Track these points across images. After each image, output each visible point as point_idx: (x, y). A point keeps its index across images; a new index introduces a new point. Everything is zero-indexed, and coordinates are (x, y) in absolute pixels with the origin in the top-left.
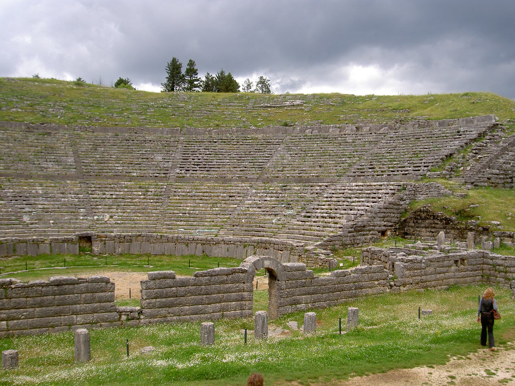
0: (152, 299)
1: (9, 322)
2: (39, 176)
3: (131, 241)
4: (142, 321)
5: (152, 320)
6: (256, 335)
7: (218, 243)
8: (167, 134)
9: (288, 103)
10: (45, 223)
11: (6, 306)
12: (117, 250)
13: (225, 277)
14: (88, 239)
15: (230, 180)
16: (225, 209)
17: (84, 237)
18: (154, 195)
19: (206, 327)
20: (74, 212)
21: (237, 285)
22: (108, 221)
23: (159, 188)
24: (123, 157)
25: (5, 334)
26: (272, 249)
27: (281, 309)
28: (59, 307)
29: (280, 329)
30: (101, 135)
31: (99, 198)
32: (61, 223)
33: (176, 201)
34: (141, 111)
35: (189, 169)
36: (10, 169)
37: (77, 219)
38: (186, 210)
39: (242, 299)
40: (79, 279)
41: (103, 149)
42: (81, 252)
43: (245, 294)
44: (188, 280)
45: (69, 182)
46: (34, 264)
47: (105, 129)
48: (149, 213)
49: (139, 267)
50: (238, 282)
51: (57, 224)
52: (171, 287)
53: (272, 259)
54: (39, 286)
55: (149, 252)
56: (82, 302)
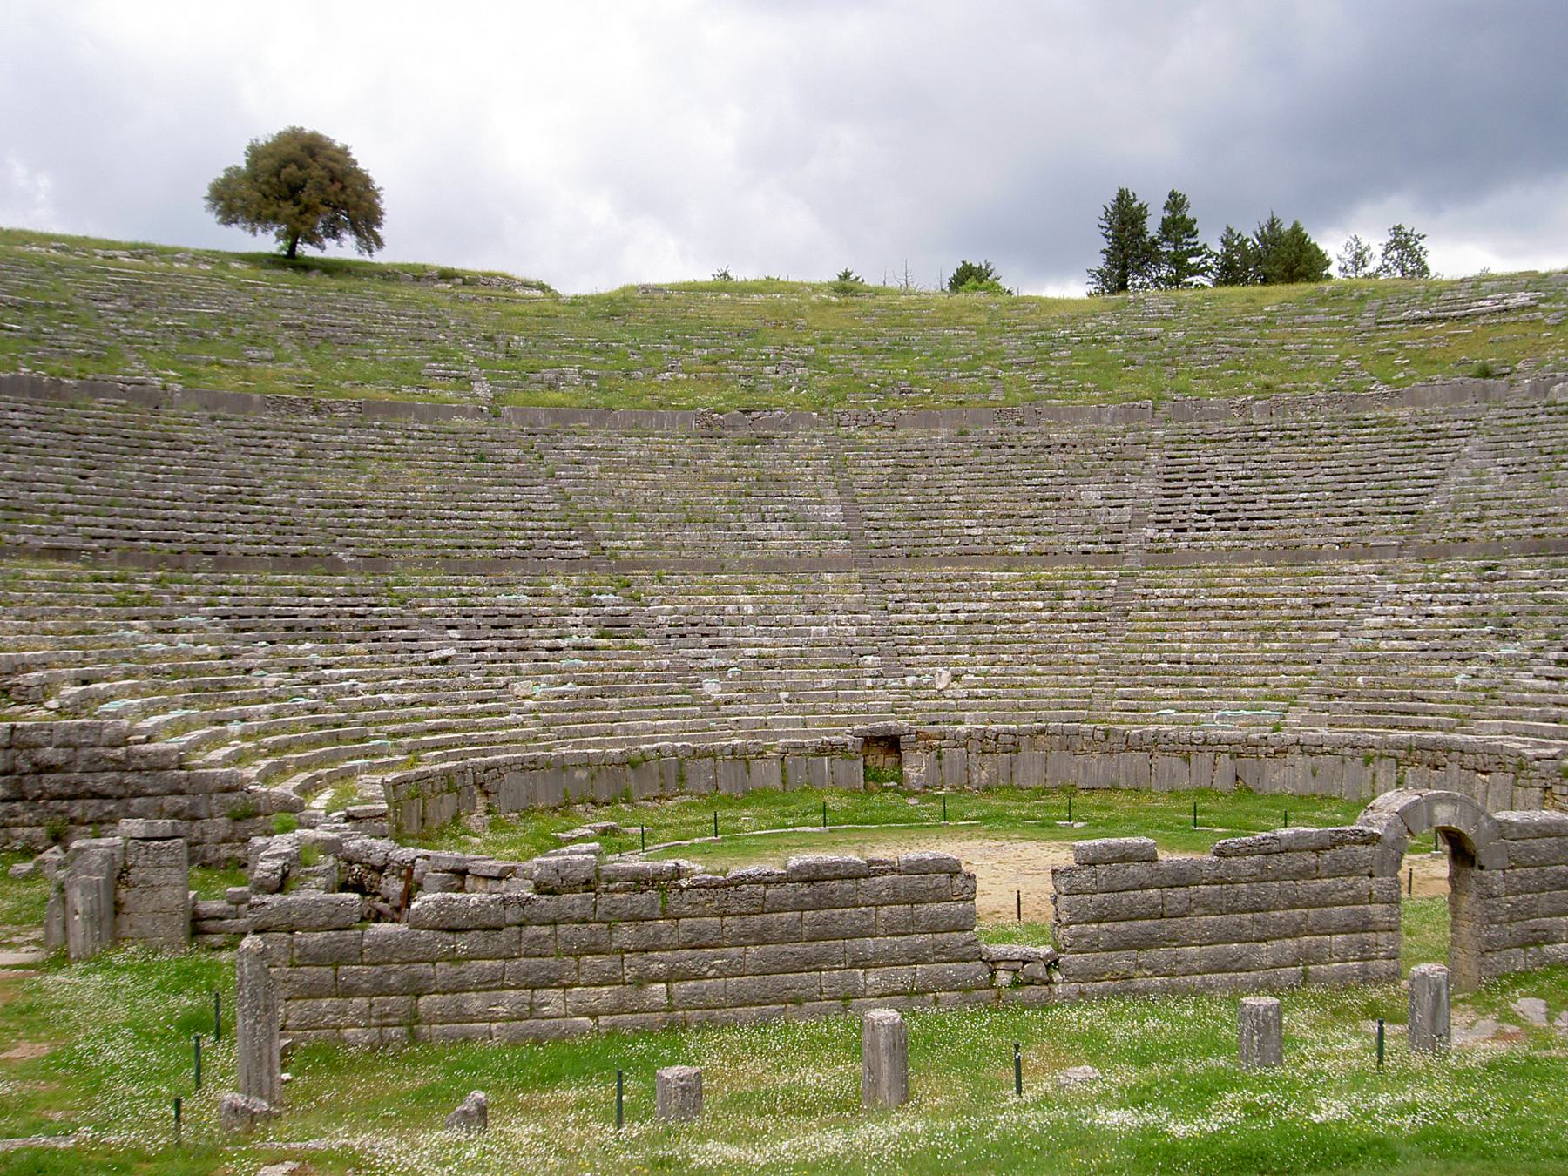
0: (1087, 922)
2: (744, 563)
3: (1016, 748)
4: (1058, 989)
5: (1088, 987)
6: (1412, 1039)
7: (1281, 751)
8: (1113, 423)
9: (1488, 303)
10: (764, 700)
12: (975, 776)
13: (1311, 858)
14: (890, 743)
15: (1315, 555)
16: (1300, 646)
17: (877, 740)
18: (1082, 609)
19: (1254, 1013)
20: (848, 666)
21: (1350, 881)
22: (947, 689)
23: (1095, 587)
24: (985, 497)
25: (664, 1022)
26: (1455, 767)
27: (1492, 958)
28: (814, 945)
29: (1488, 1023)
30: (917, 434)
31: (919, 623)
32: (809, 697)
33: (1153, 625)
34: (1032, 358)
35: (1185, 525)
36: (660, 547)
37: (856, 686)
38: (1180, 651)
39: (1366, 925)
40: (871, 863)
41: (924, 477)
42: (871, 784)
43: (1376, 910)
44: (1196, 867)
45: (829, 577)
46: (737, 819)
47: (927, 418)
48: (1067, 662)
49: (1043, 826)
50: (1351, 872)
51: (798, 701)
52: (1143, 887)
53: (1461, 800)
54: (758, 882)
55: (1071, 781)
56: (881, 931)
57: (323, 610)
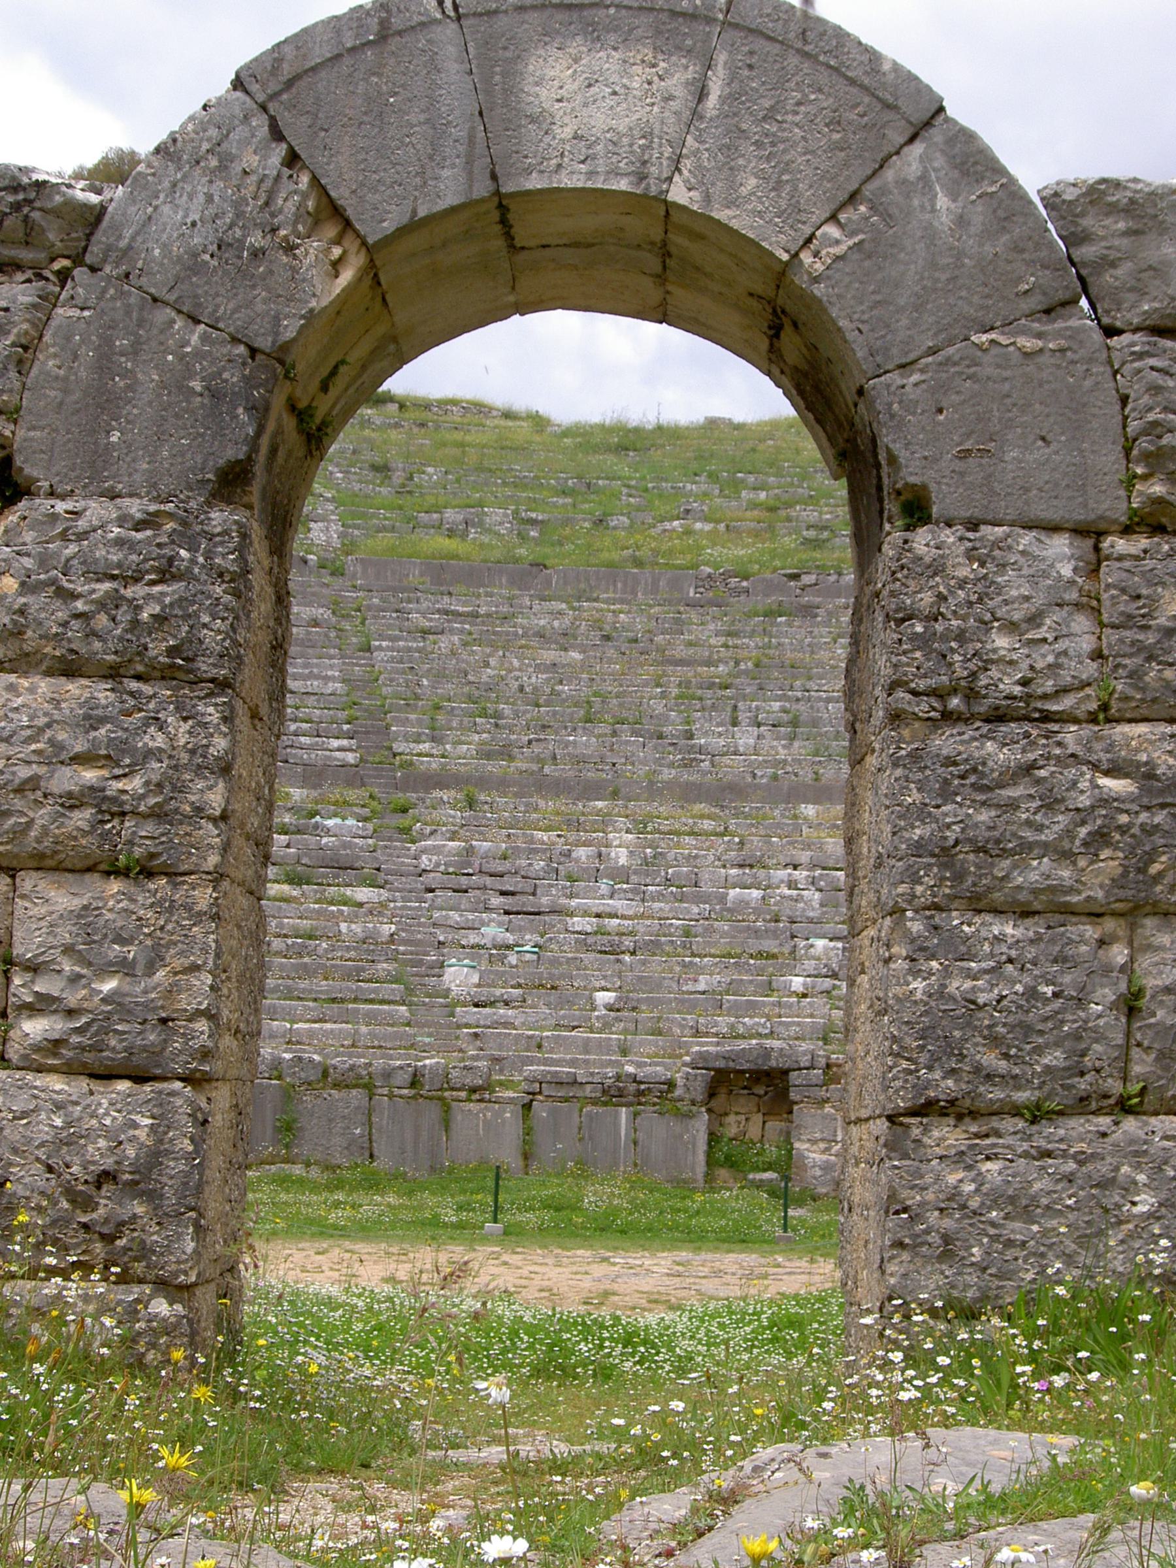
37: (769, 988)
42: (723, 1173)
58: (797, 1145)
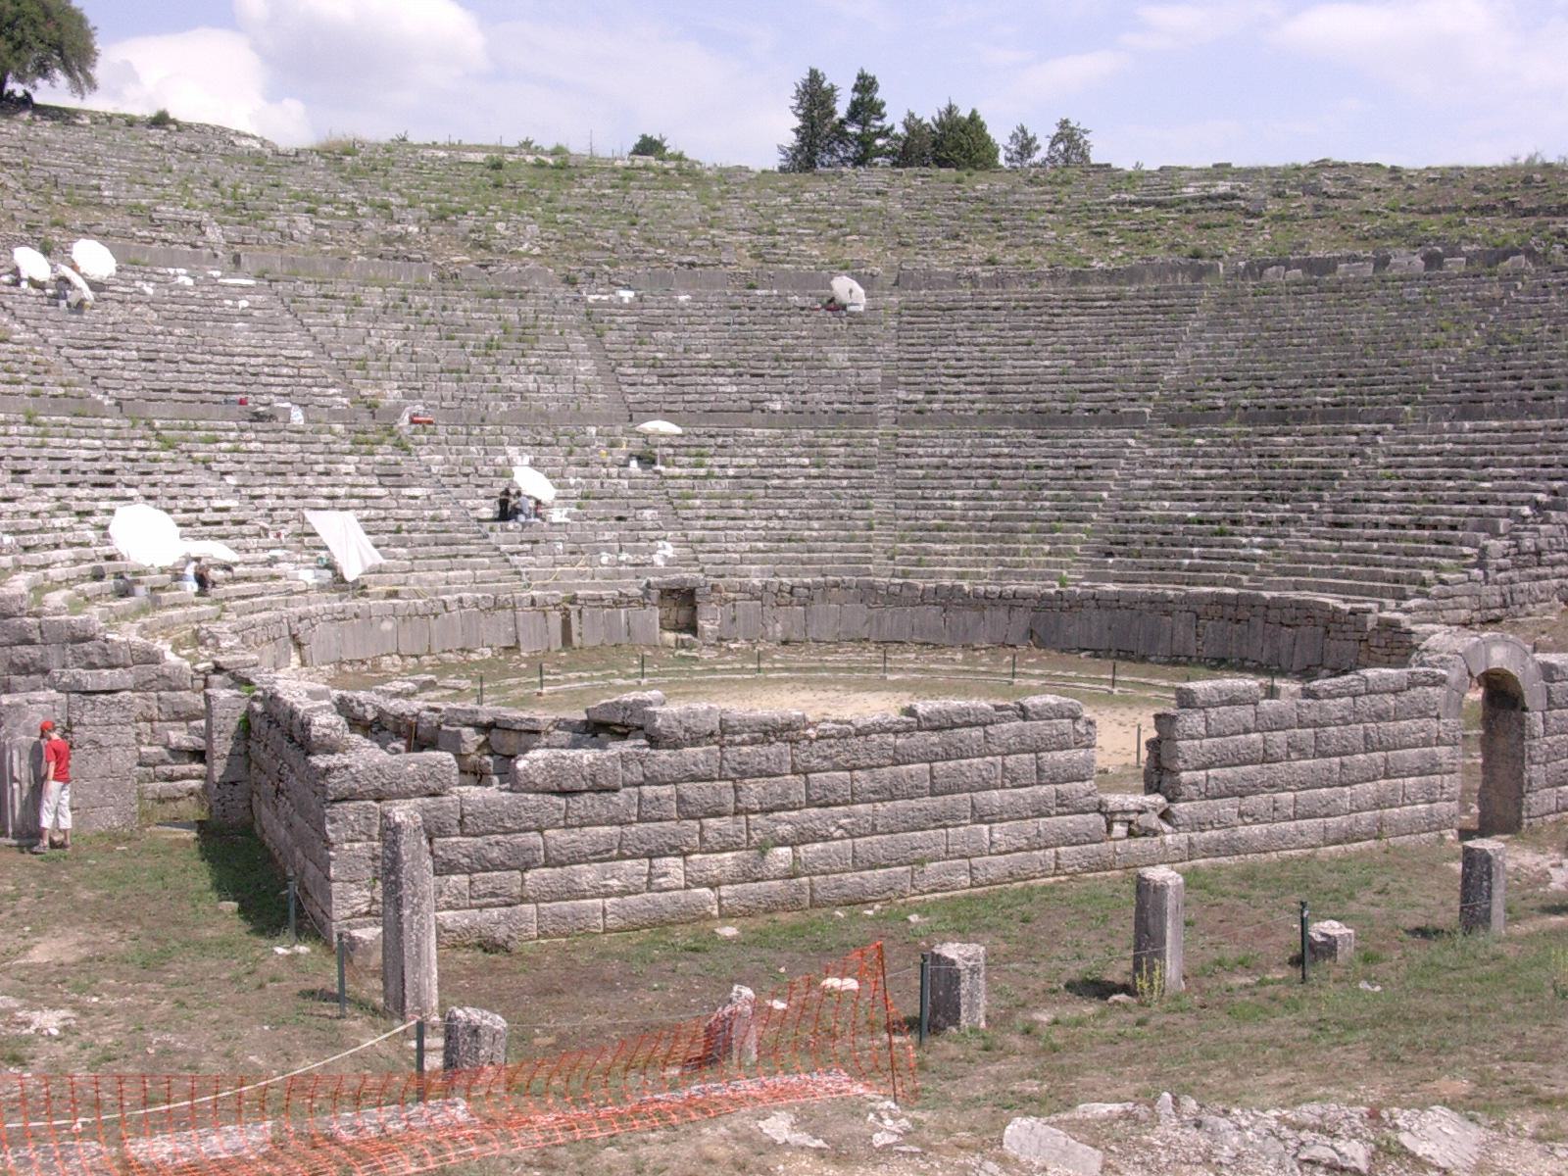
0: (1197, 769)
1: (801, 849)
9: (1191, 190)
11: (792, 798)
12: (770, 629)
26: (1260, 622)
52: (1247, 731)
54: (887, 731)
57: (96, 454)
58: (700, 622)
